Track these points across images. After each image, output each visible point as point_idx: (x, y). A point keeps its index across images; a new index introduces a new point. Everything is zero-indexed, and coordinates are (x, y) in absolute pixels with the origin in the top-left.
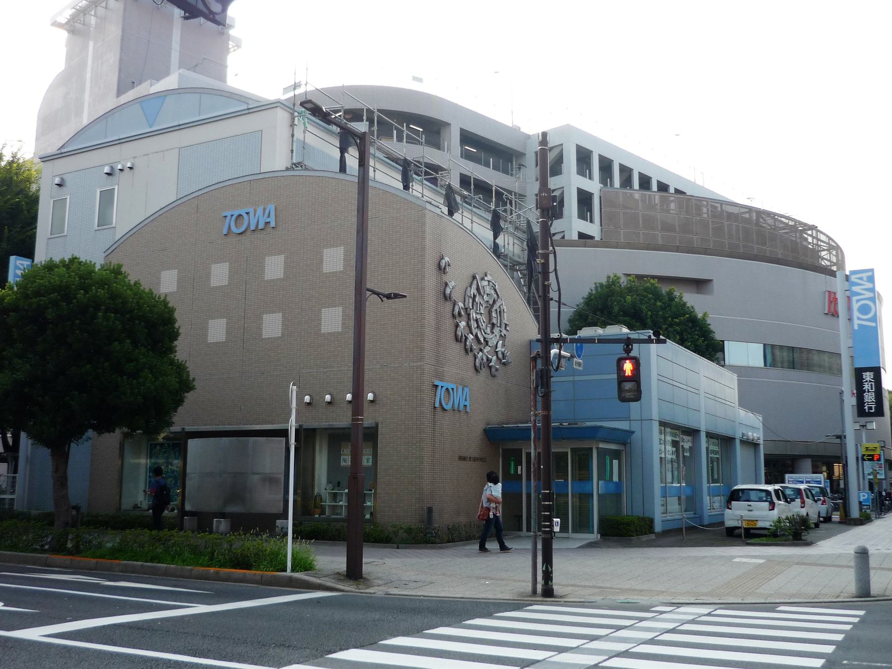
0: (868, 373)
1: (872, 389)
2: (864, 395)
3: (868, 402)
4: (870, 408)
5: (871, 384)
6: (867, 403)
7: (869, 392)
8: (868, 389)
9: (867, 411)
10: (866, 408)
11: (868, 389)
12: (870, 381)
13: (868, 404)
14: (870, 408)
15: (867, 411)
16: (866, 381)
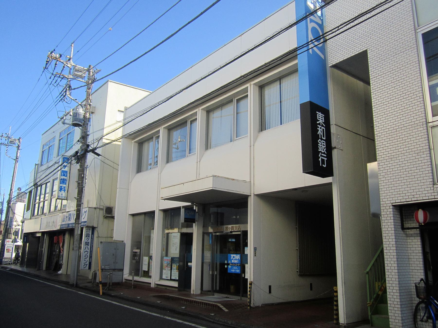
0: (320, 113)
1: (324, 137)
2: (319, 141)
3: (321, 152)
4: (323, 160)
5: (323, 129)
6: (320, 153)
7: (322, 139)
8: (321, 135)
9: (321, 165)
10: (320, 159)
11: (321, 135)
12: (322, 126)
13: (321, 156)
14: (323, 160)
15: (321, 165)
16: (319, 124)
